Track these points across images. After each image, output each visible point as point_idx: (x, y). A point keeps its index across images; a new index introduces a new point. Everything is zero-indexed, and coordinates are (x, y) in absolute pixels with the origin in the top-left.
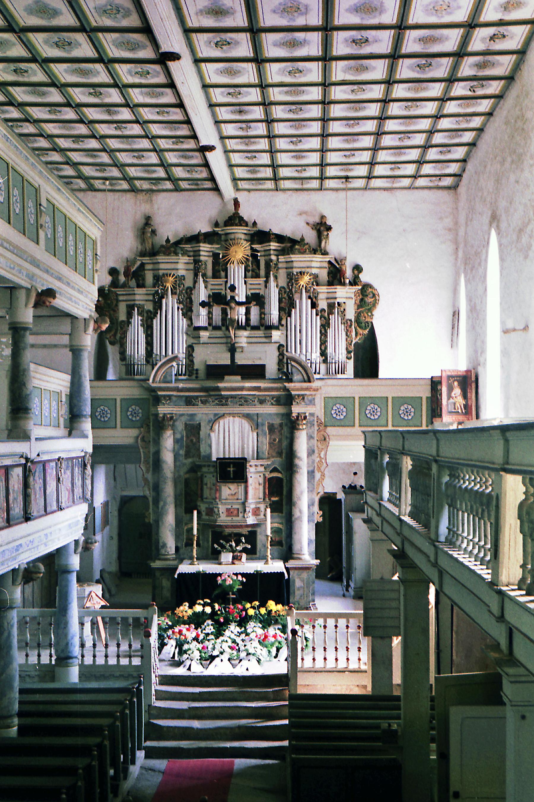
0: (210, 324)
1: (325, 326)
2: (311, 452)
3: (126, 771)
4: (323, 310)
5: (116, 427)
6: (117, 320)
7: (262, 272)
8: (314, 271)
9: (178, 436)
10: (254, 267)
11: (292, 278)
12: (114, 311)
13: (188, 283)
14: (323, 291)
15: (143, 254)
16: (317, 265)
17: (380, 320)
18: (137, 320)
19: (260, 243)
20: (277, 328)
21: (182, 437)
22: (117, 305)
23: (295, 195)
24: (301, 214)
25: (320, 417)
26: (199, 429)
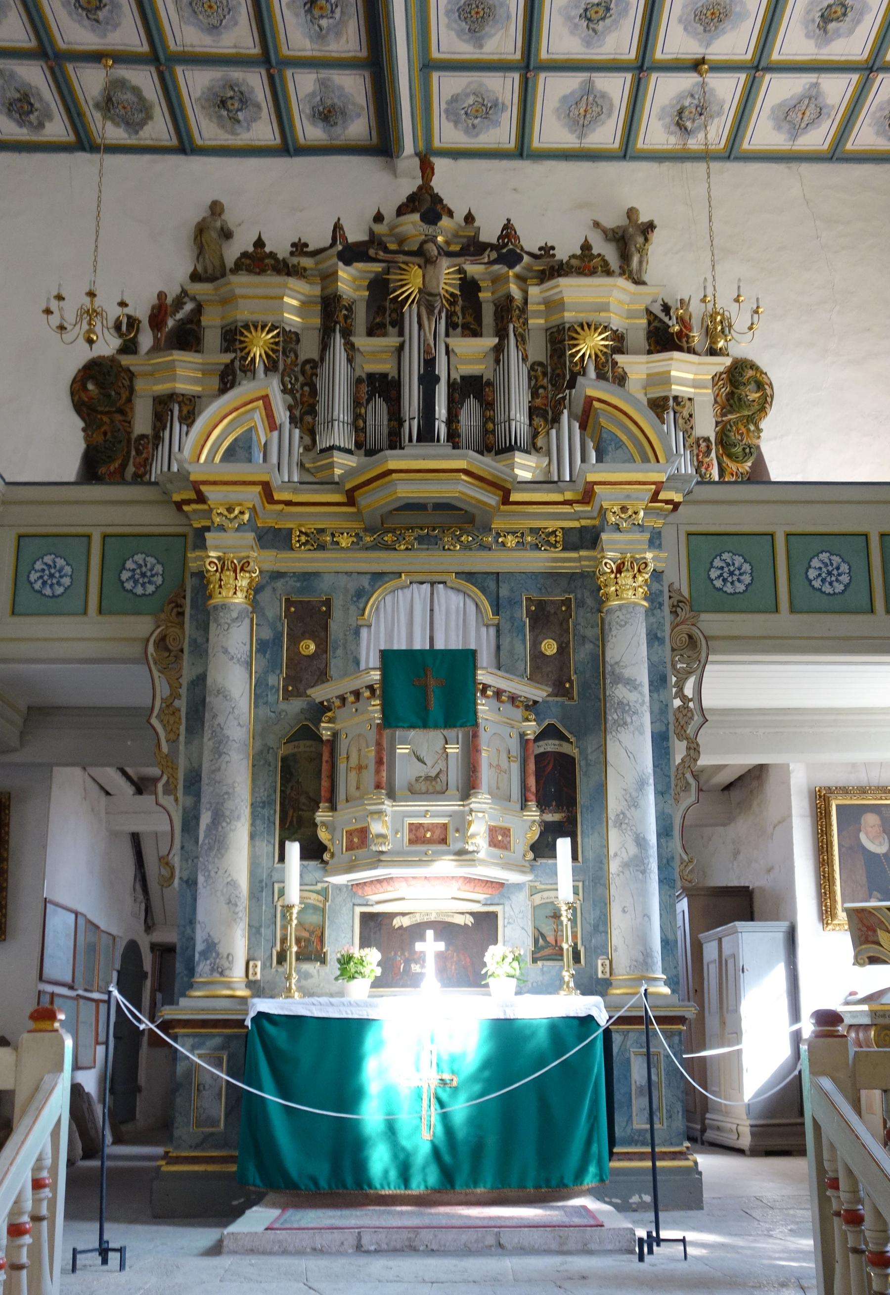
0: (358, 445)
2: (658, 681)
5: (85, 613)
6: (129, 433)
8: (617, 322)
9: (267, 634)
11: (560, 338)
12: (122, 412)
13: (308, 349)
14: (637, 366)
15: (195, 277)
21: (278, 637)
22: (129, 400)
25: (676, 586)
26: (328, 614)
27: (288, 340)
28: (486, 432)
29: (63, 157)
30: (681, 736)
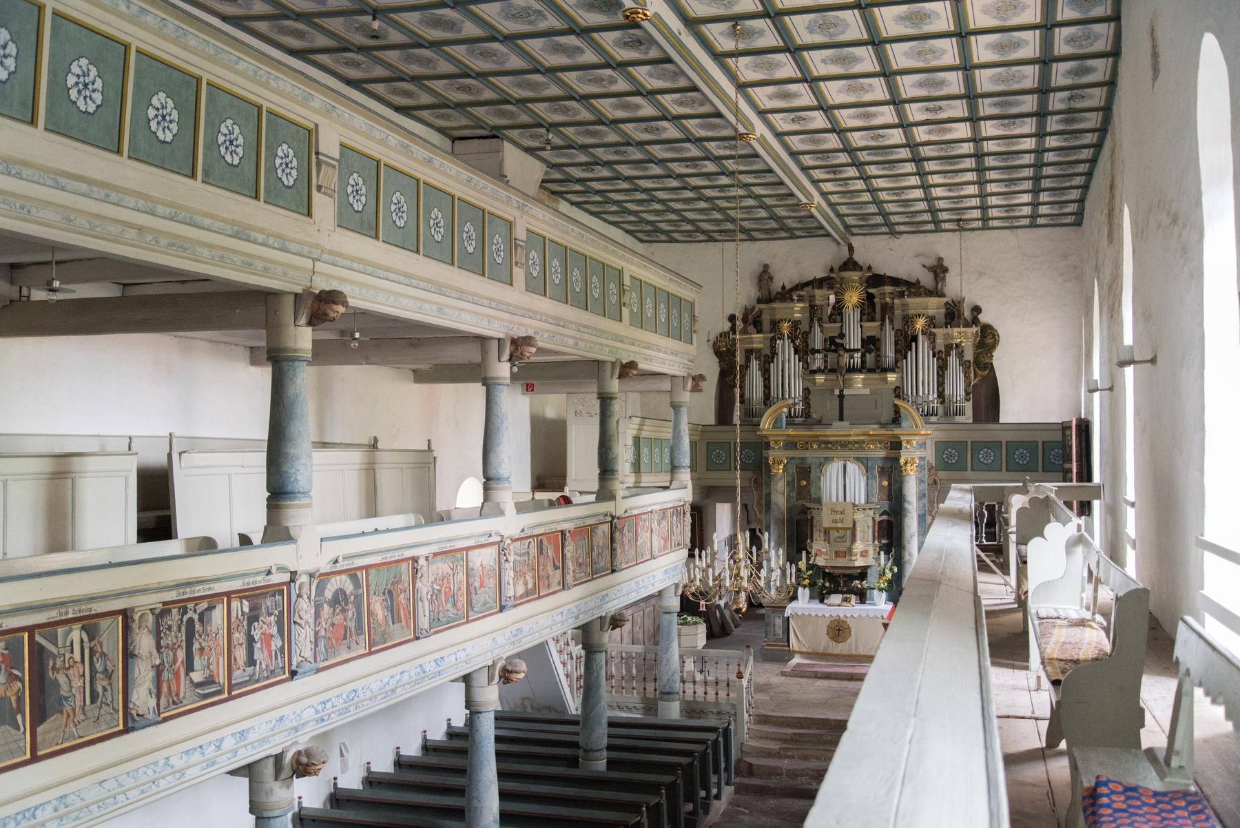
1: (942, 368)
3: (706, 809)
4: (940, 352)
7: (878, 316)
8: (931, 312)
10: (869, 308)
11: (908, 320)
15: (759, 301)
16: (934, 306)
17: (1001, 360)
18: (754, 364)
19: (875, 287)
20: (893, 370)
23: (911, 236)
24: (917, 256)
27: (796, 324)
28: (878, 361)
29: (702, 244)
30: (930, 514)
